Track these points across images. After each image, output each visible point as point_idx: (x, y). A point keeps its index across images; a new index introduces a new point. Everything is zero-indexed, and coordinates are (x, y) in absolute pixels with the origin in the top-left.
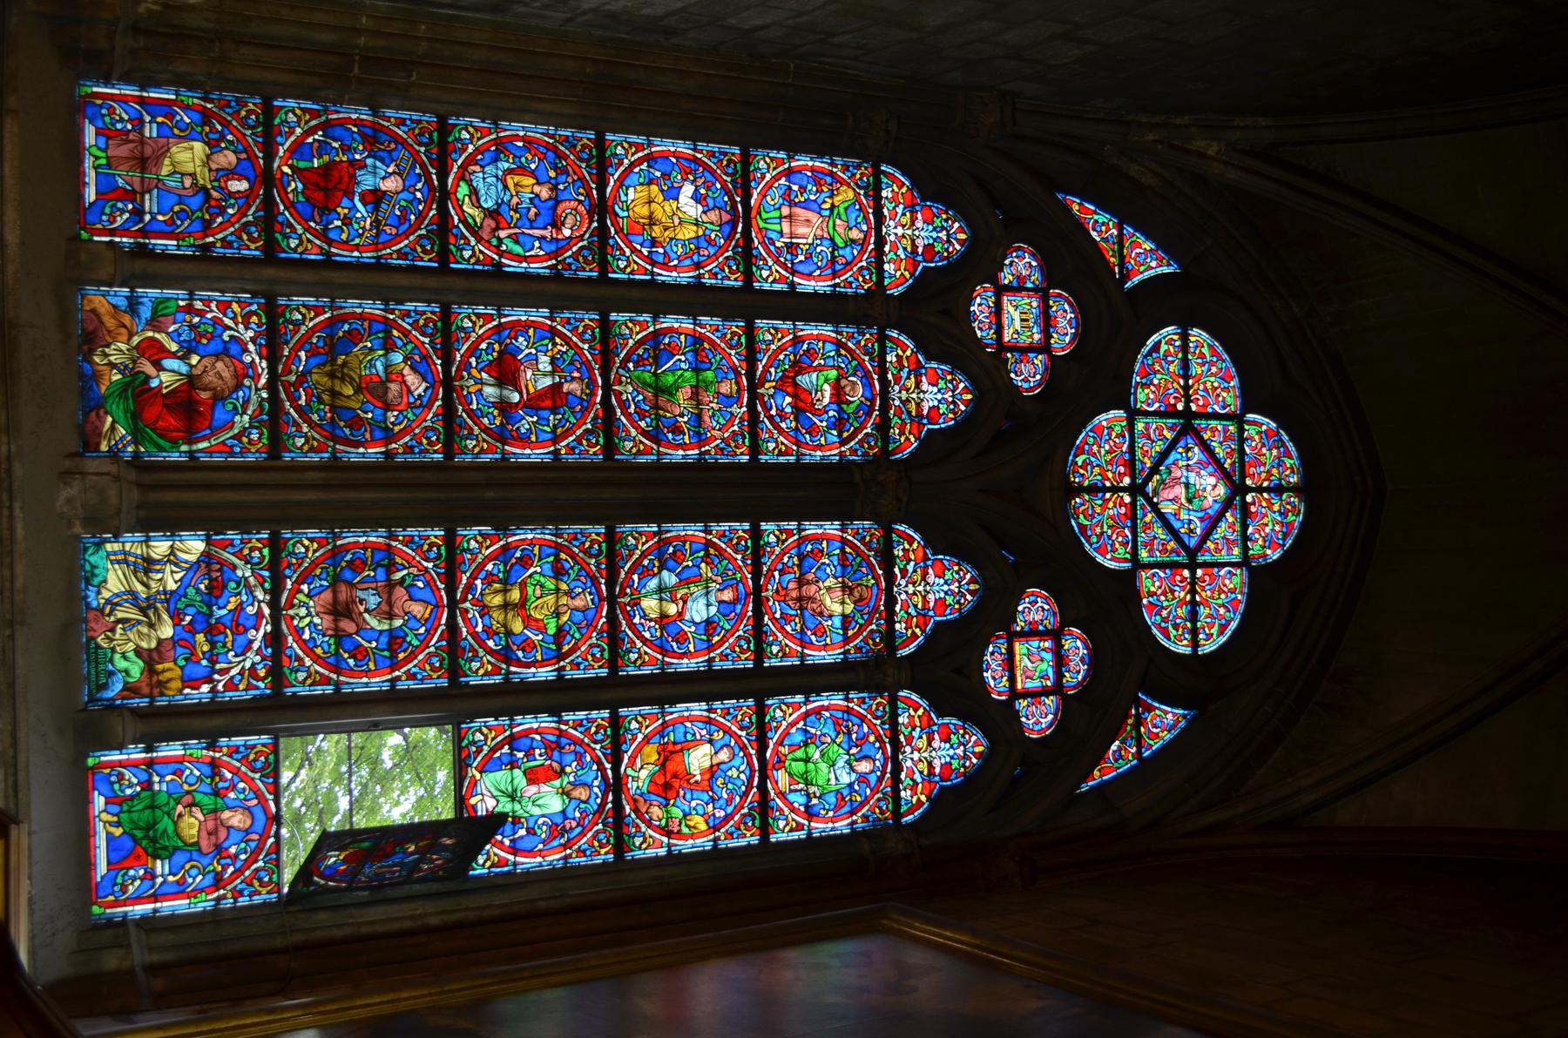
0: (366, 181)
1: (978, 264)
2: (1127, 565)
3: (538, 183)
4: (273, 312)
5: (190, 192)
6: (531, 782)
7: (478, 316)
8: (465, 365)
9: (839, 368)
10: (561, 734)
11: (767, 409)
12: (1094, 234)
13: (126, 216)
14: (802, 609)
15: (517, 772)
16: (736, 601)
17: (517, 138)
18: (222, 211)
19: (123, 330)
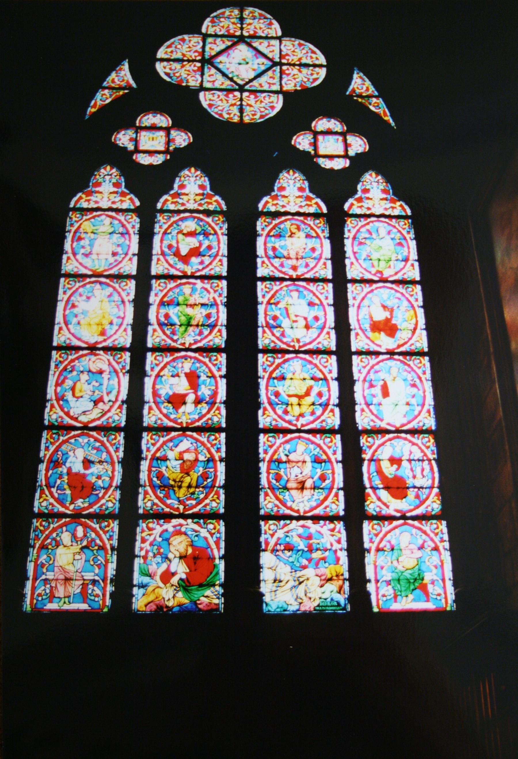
0: (78, 467)
1: (123, 160)
2: (281, 97)
3: (79, 380)
4: (147, 516)
5: (83, 556)
7: (149, 413)
8: (174, 421)
9: (178, 233)
11: (199, 270)
12: (108, 101)
13: (95, 588)
14: (302, 258)
16: (297, 290)
17: (55, 391)
18: (93, 540)
19: (156, 590)
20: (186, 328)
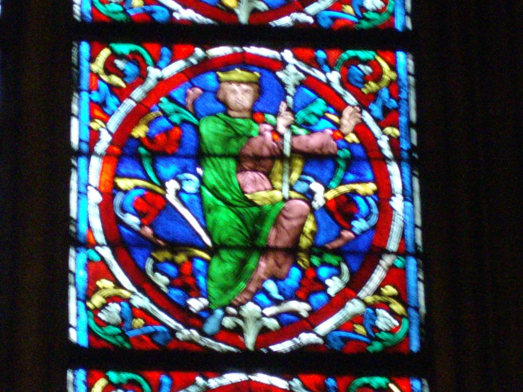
20: (243, 263)
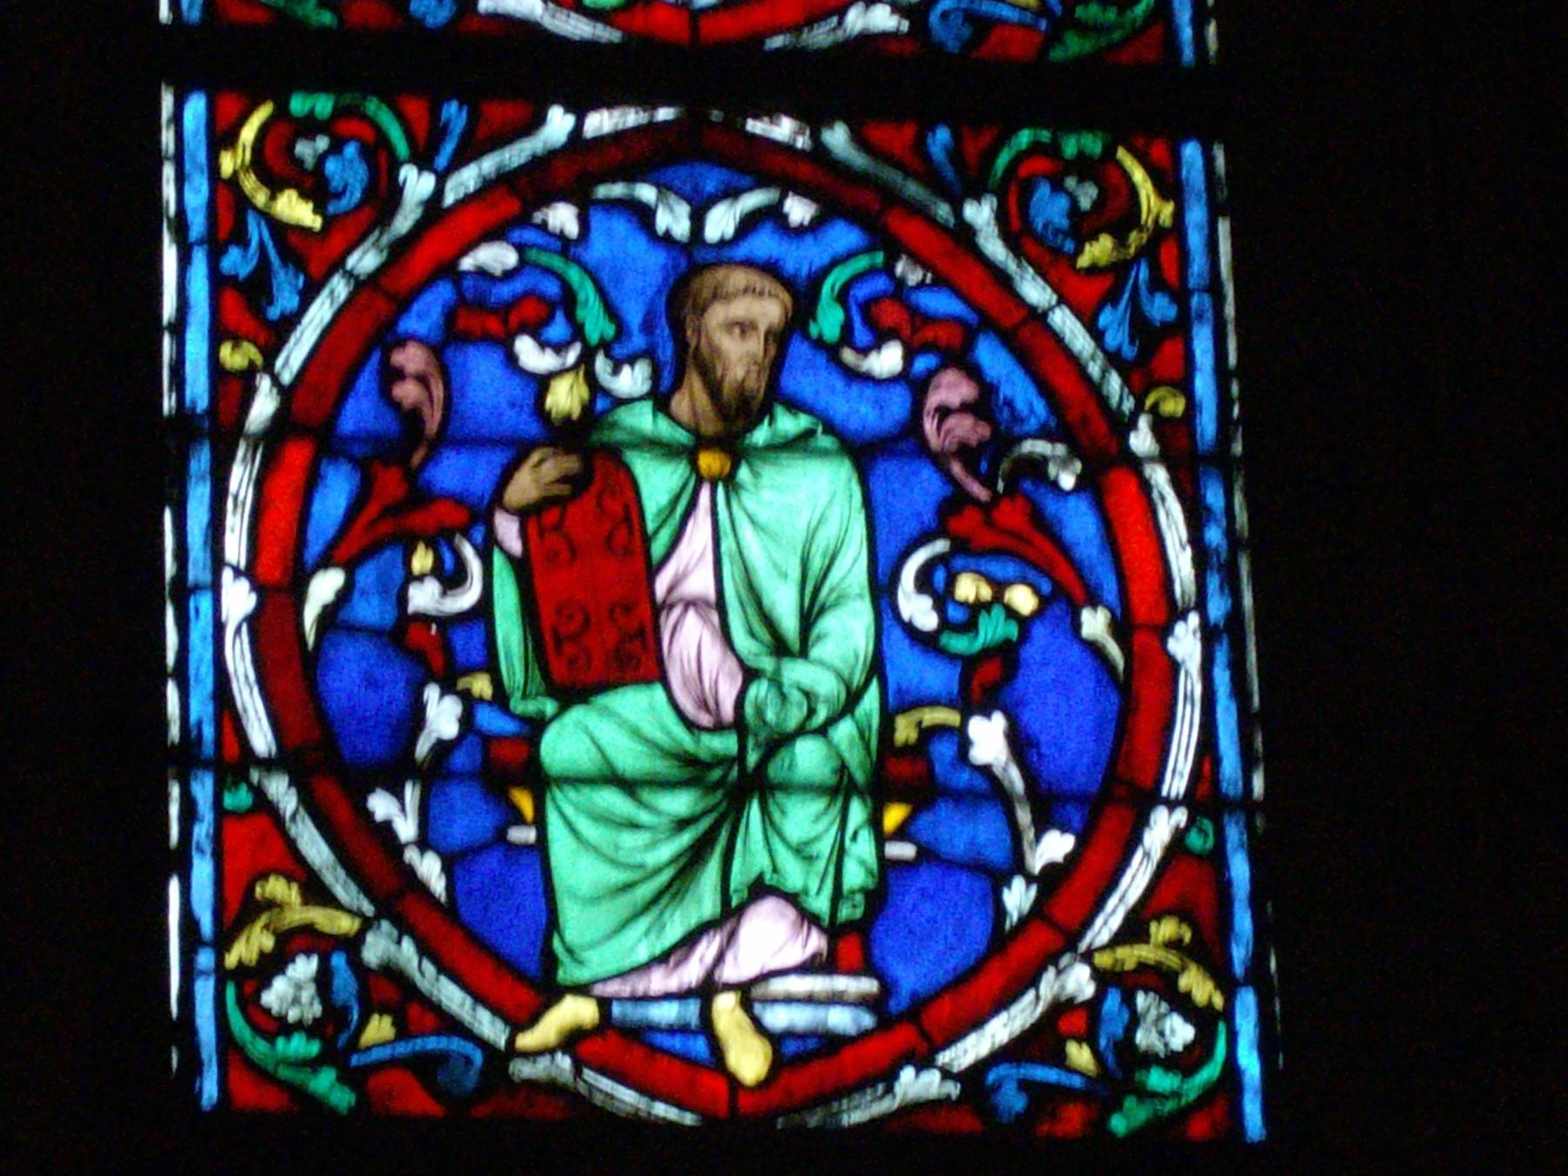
6: (640, 660)
10: (307, 424)
15: (566, 743)
